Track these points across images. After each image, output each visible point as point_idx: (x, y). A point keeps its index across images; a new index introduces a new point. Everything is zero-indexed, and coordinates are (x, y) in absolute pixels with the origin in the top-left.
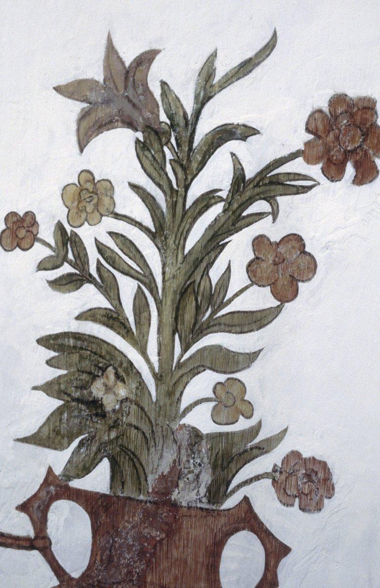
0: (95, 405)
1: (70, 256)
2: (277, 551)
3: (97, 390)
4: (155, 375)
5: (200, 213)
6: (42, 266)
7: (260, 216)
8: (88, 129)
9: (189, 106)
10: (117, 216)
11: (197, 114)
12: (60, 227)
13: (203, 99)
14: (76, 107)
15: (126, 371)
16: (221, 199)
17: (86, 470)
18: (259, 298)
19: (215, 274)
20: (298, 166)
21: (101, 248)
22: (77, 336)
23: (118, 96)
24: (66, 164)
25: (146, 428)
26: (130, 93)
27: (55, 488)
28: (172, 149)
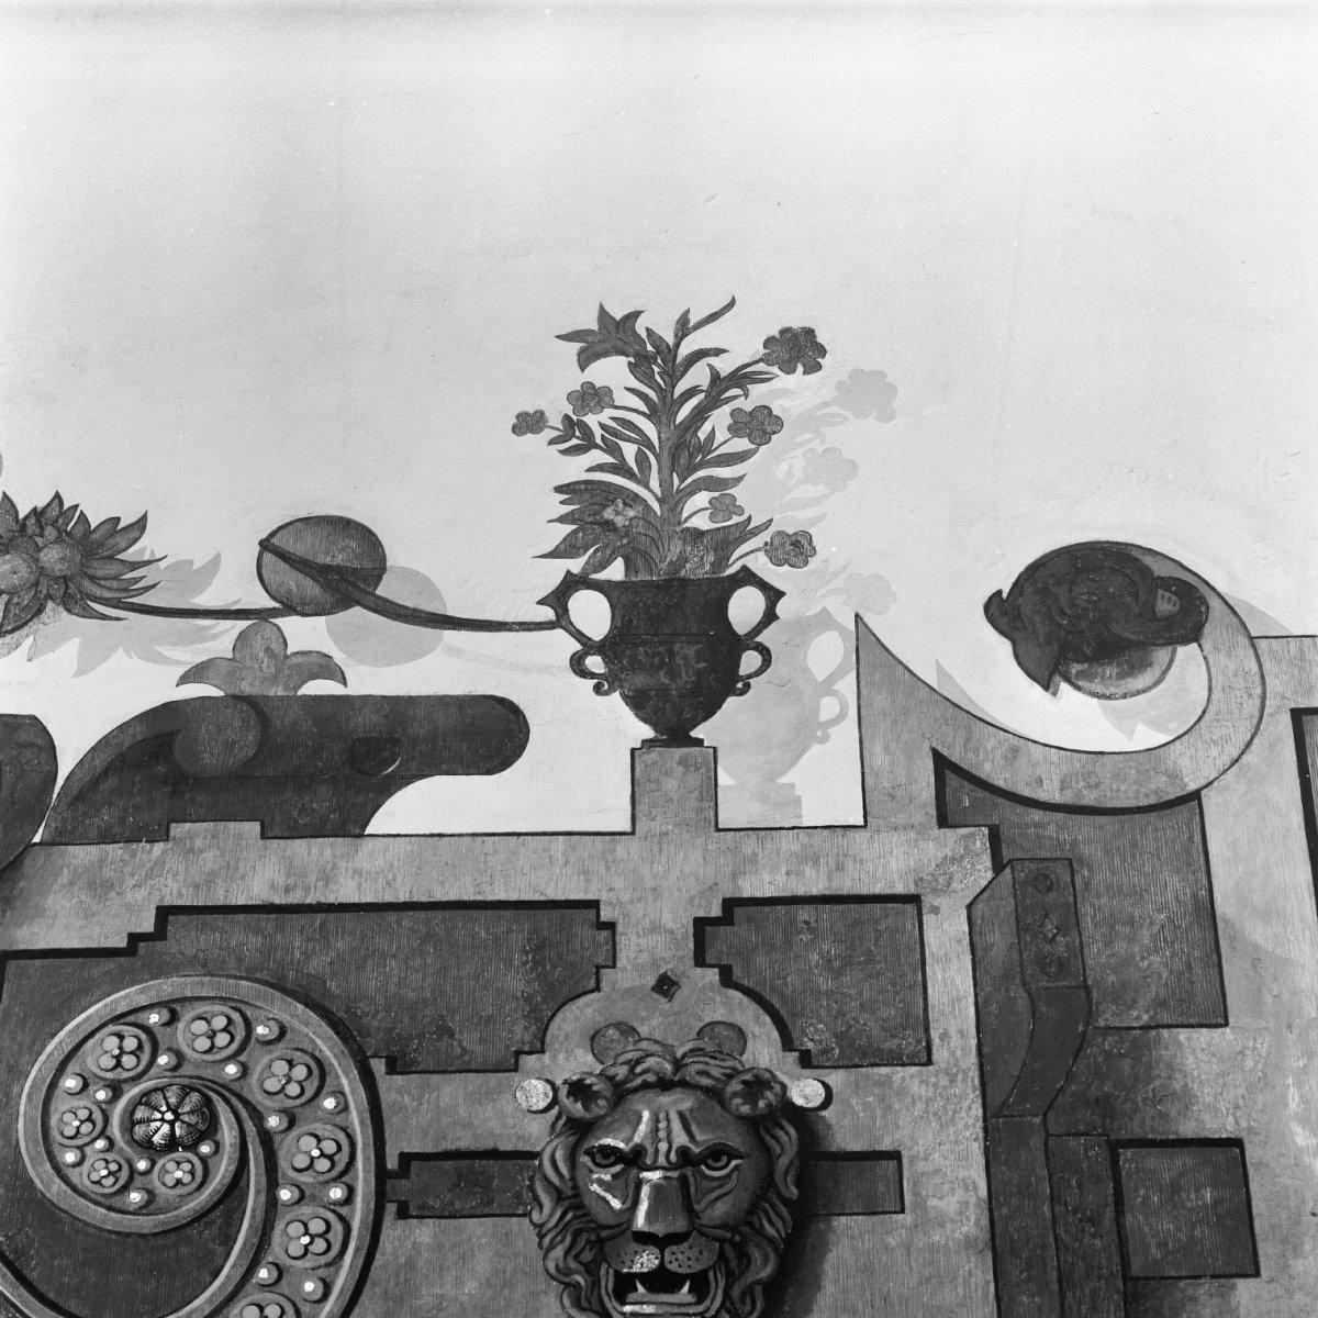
0: (609, 526)
1: (577, 433)
2: (773, 595)
3: (608, 514)
4: (658, 499)
5: (687, 400)
6: (552, 442)
7: (735, 397)
8: (585, 360)
9: (670, 340)
10: (616, 407)
11: (677, 345)
12: (567, 417)
13: (679, 340)
14: (574, 347)
15: (632, 499)
16: (702, 391)
17: (603, 566)
18: (742, 444)
19: (702, 434)
20: (761, 367)
21: (603, 427)
22: (586, 482)
23: (612, 334)
24: (575, 379)
25: (653, 534)
26: (621, 335)
27: (571, 584)
28: (659, 366)
